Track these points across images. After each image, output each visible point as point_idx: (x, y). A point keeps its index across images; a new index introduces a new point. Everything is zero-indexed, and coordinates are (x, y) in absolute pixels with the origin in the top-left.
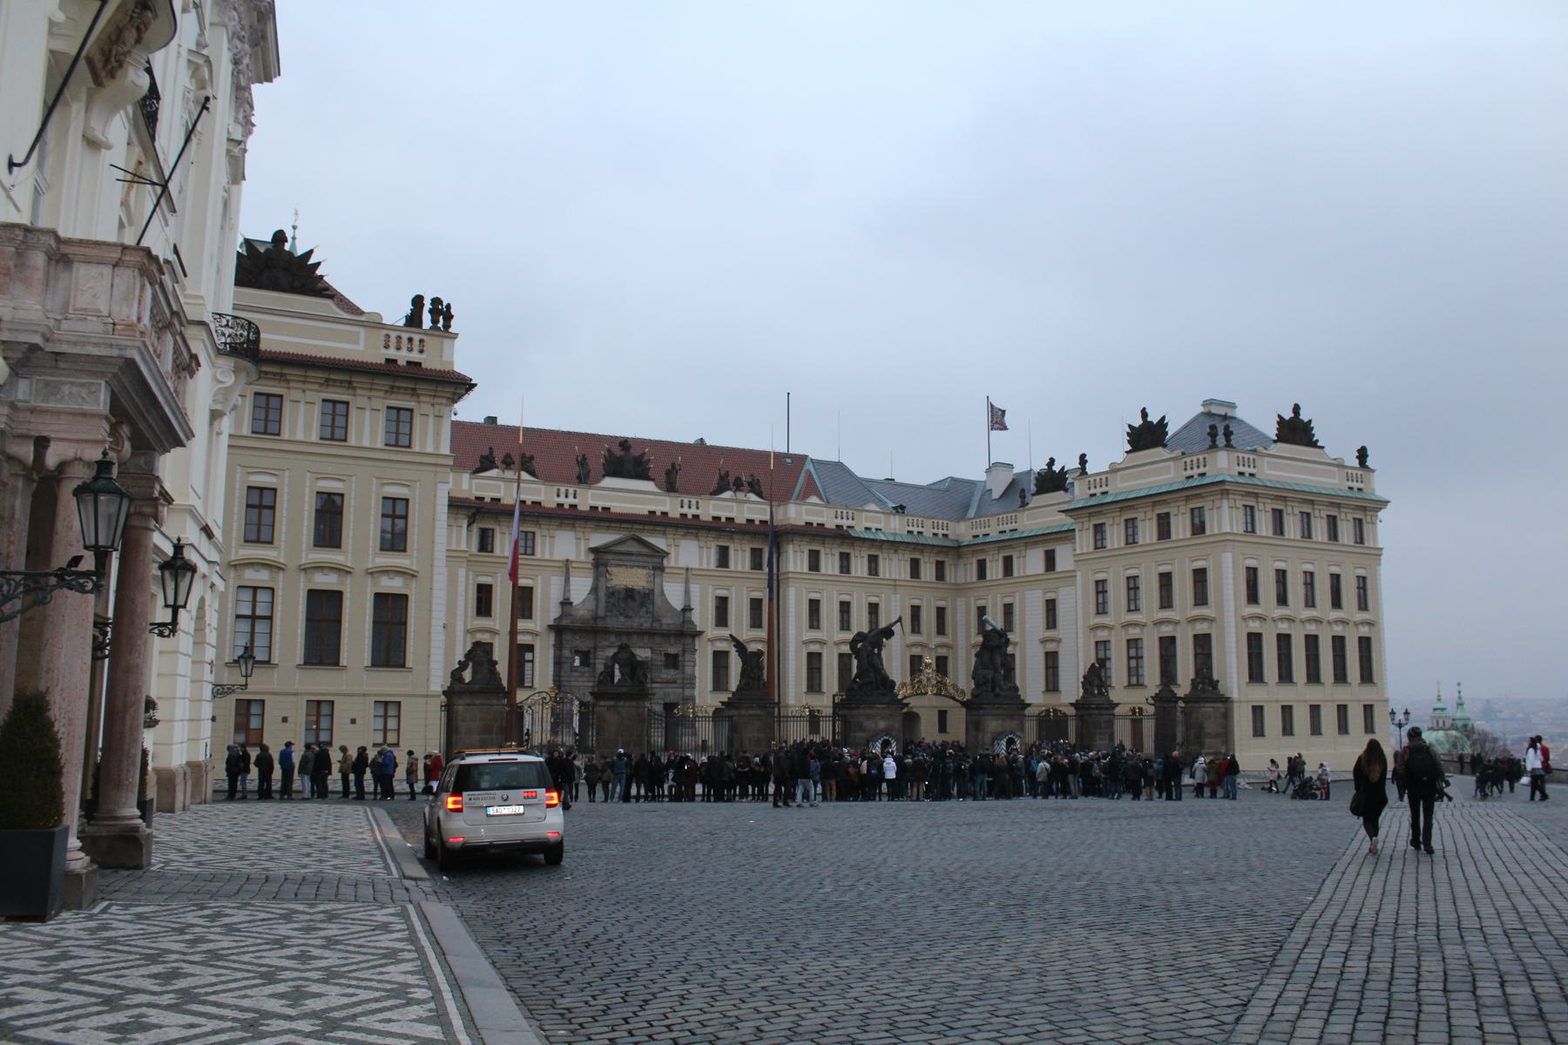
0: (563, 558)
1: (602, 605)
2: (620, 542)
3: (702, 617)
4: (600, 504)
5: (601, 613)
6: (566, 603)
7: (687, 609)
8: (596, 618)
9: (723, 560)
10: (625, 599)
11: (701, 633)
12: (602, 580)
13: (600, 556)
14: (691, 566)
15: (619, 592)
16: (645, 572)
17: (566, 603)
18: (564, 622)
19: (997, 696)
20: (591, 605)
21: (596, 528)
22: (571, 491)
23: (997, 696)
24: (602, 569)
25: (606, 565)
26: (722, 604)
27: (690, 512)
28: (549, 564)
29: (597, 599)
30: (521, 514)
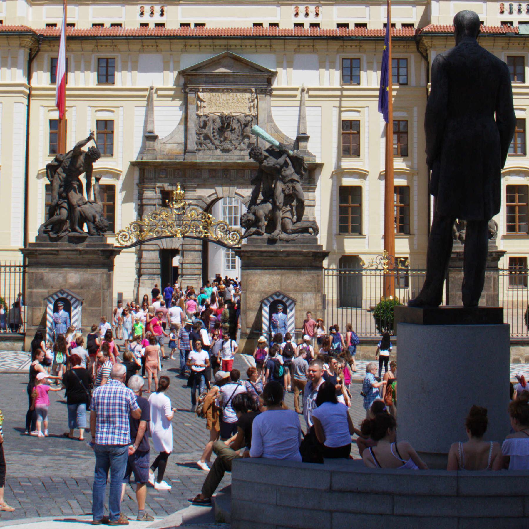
0: (147, 86)
1: (193, 138)
2: (215, 63)
3: (322, 148)
4: (192, 21)
5: (192, 146)
6: (150, 137)
7: (302, 138)
8: (186, 151)
9: (351, 75)
10: (222, 130)
11: (321, 166)
12: (192, 108)
13: (190, 81)
14: (306, 86)
15: (214, 121)
16: (248, 95)
17: (150, 137)
18: (145, 159)
19: (272, 241)
20: (181, 138)
21: (185, 50)
22: (157, 9)
23: (272, 241)
24: (191, 96)
25: (196, 91)
26: (350, 131)
27: (307, 22)
28: (131, 94)
29: (186, 130)
30: (70, 39)
